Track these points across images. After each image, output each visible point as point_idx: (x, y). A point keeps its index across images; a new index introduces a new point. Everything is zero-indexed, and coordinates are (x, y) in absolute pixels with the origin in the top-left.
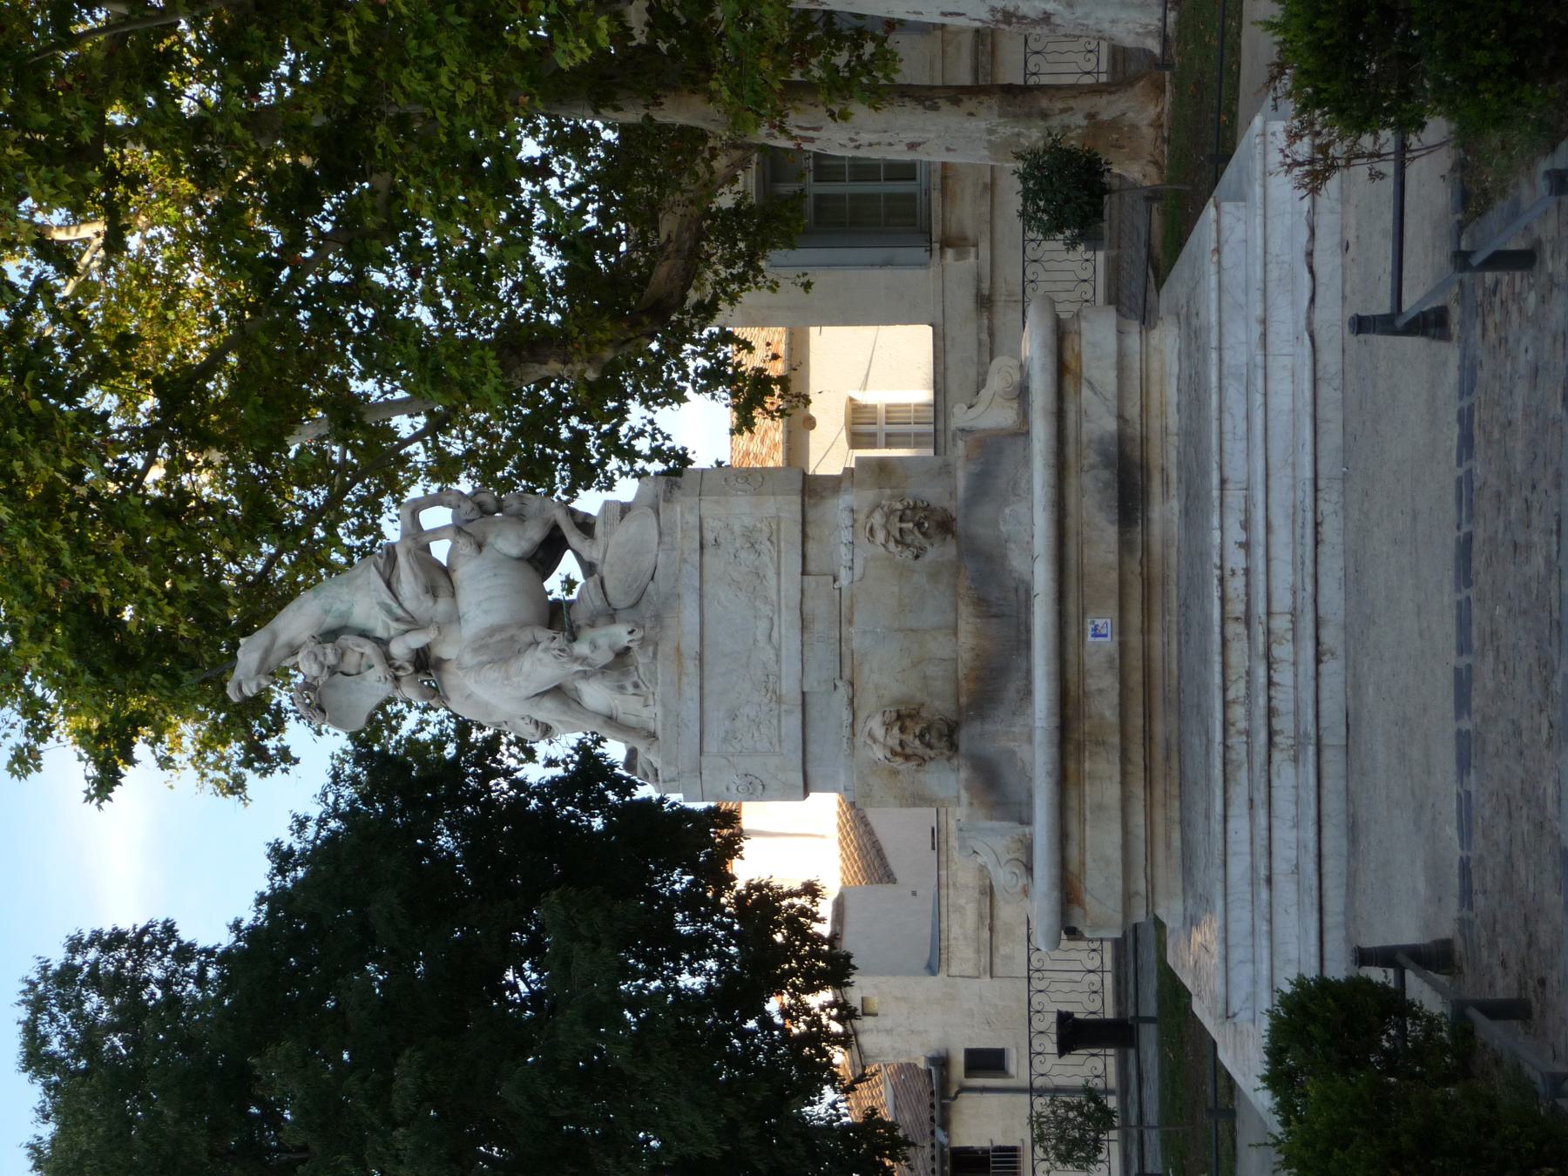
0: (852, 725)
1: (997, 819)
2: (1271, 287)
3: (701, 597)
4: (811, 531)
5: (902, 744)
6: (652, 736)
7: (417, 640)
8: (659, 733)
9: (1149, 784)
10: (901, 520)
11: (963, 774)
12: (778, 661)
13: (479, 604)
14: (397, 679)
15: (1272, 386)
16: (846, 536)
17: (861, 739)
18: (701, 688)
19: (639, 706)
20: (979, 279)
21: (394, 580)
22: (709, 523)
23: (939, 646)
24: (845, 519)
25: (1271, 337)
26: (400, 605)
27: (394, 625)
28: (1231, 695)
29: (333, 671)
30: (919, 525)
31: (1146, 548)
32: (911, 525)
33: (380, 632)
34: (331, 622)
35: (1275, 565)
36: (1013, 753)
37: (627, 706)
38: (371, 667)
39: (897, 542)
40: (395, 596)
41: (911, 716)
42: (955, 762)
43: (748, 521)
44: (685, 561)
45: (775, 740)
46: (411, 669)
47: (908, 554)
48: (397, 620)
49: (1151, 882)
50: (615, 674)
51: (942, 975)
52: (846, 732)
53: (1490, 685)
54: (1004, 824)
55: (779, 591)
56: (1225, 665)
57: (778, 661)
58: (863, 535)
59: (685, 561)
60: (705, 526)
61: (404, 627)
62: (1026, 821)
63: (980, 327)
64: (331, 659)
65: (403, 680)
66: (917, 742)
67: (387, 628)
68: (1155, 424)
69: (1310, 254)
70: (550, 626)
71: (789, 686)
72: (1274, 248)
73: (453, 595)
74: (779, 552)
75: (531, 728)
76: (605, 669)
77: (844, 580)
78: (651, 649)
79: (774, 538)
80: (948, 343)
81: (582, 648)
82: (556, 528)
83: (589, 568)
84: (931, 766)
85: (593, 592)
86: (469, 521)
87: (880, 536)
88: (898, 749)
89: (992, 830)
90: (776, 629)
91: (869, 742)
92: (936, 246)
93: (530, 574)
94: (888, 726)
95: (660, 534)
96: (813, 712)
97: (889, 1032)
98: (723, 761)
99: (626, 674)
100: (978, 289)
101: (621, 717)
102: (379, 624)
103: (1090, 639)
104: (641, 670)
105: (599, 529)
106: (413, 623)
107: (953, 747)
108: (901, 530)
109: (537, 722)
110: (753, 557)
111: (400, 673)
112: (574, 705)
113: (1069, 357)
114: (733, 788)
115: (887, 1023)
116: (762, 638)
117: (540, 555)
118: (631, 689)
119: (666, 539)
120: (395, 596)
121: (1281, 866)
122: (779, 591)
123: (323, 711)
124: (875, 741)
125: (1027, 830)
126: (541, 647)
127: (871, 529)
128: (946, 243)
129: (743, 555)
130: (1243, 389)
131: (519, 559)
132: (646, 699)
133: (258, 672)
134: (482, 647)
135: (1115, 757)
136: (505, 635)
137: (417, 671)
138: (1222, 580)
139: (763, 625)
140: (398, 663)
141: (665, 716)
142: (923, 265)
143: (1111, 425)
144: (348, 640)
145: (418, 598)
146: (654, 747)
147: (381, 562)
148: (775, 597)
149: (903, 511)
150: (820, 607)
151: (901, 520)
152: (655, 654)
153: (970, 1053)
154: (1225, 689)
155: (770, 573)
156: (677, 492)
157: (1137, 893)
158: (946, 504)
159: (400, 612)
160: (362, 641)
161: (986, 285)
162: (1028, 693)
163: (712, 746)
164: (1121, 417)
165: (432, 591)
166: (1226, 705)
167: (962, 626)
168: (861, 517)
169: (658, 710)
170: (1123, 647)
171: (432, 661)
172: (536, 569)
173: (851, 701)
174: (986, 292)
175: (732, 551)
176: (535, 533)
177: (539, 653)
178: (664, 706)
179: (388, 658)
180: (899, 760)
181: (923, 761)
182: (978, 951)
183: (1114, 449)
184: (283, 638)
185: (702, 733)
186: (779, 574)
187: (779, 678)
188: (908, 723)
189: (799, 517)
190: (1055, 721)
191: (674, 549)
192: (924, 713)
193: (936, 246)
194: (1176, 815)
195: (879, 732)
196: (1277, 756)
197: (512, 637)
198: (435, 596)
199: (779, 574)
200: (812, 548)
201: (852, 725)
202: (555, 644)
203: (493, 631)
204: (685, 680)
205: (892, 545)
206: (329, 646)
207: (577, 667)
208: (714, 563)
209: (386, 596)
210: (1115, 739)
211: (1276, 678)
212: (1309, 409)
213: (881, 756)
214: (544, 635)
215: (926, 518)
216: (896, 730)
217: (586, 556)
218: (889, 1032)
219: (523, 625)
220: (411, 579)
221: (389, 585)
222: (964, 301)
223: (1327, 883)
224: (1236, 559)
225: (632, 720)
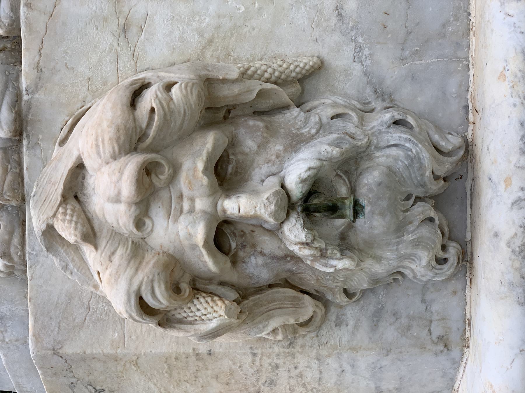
5: (224, 235)
88: (208, 263)
91: (67, 231)
94: (149, 150)
180: (212, 312)
195: (111, 188)
213: (117, 296)
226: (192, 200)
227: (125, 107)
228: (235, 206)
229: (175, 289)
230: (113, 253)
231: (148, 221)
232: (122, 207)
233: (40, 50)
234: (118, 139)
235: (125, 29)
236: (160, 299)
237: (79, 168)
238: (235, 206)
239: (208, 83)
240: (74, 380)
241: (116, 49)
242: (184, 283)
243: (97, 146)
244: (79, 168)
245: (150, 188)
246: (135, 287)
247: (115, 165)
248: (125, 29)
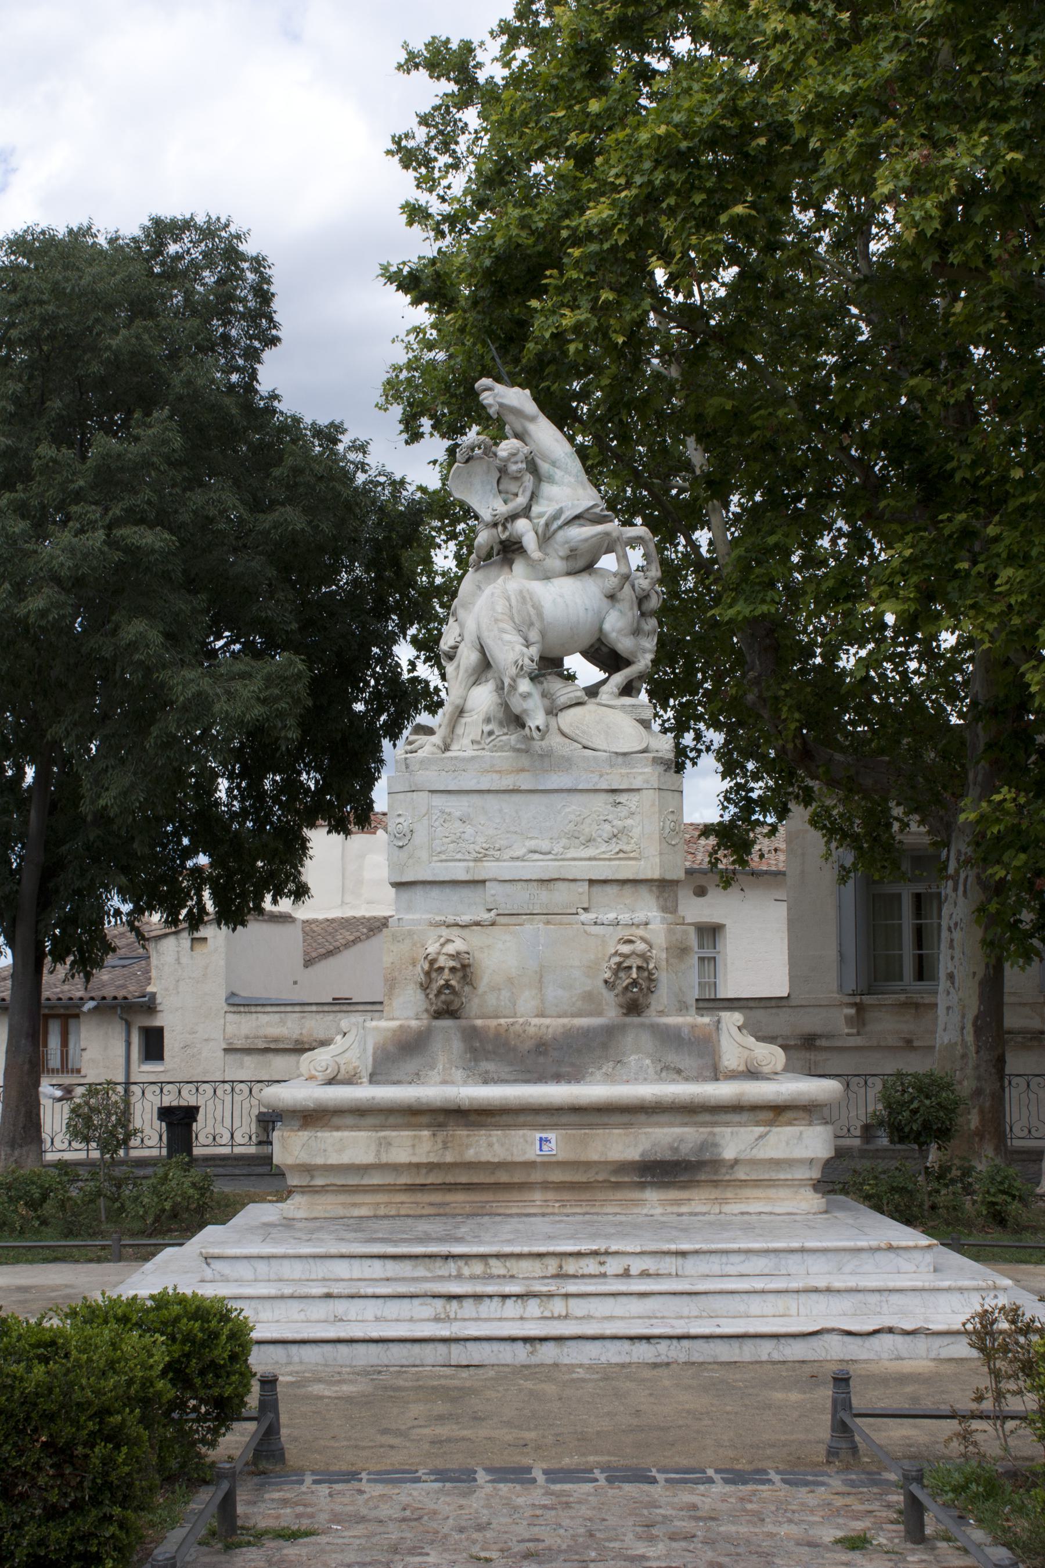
0: (457, 925)
1: (374, 1053)
2: (860, 1296)
3: (569, 791)
4: (628, 890)
5: (441, 969)
6: (447, 748)
7: (530, 542)
8: (448, 754)
9: (411, 1188)
10: (639, 968)
11: (414, 1023)
12: (512, 859)
13: (562, 596)
14: (495, 525)
15: (771, 1298)
16: (625, 917)
17: (445, 932)
18: (489, 791)
19: (471, 737)
20: (829, 1036)
21: (582, 521)
22: (635, 798)
23: (526, 1002)
24: (640, 916)
25: (814, 1296)
26: (560, 527)
27: (542, 521)
28: (493, 1262)
29: (503, 471)
30: (635, 983)
31: (617, 1186)
32: (634, 976)
33: (536, 509)
34: (544, 467)
35: (611, 1300)
36: (432, 1068)
37: (472, 726)
38: (506, 502)
39: (619, 964)
40: (569, 523)
42: (425, 1016)
43: (636, 832)
44: (601, 776)
45: (443, 857)
46: (503, 537)
47: (608, 975)
48: (547, 525)
49: (323, 1190)
50: (501, 715)
51: (226, 1008)
52: (451, 919)
53: (520, 1501)
54: (370, 1059)
55: (574, 859)
56: (520, 1256)
57: (512, 859)
58: (626, 933)
59: (601, 776)
60: (632, 794)
61: (540, 531)
62: (374, 1078)
63: (787, 1038)
64: (513, 468)
65: (494, 531)
66: (442, 982)
67: (540, 515)
68: (729, 1194)
69: (890, 1330)
70: (542, 658)
71: (488, 869)
72: (894, 1298)
73: (569, 574)
74: (610, 859)
75: (451, 642)
76: (506, 706)
77: (584, 917)
78: (523, 747)
79: (621, 855)
80: (774, 1011)
81: (524, 685)
82: (628, 663)
83: (592, 691)
84: (420, 996)
85: (572, 695)
86: (633, 586)
87: (625, 949)
88: (436, 966)
89: (365, 1050)
90: (541, 857)
91: (442, 940)
92: (857, 999)
93: (586, 642)
95: (625, 754)
96: (466, 892)
97: (178, 960)
98: (424, 811)
99: (501, 724)
100: (820, 1036)
101: (463, 721)
102: (543, 509)
103: (538, 1135)
104: (504, 738)
105: (627, 700)
106: (545, 538)
107: (438, 1015)
108: (630, 968)
109: (456, 647)
110: (605, 836)
111: (500, 528)
112: (473, 679)
113: (789, 1115)
114: (401, 820)
115: (184, 960)
116: (532, 844)
117: (604, 649)
118: (487, 728)
119: (620, 759)
120: (569, 523)
121: (340, 1307)
122: (574, 859)
123: (467, 461)
124: (442, 945)
125: (365, 1080)
126: (525, 649)
127: (631, 942)
128: (860, 1007)
129: (607, 827)
130: (766, 1271)
131: (601, 630)
132: (478, 743)
133: (501, 405)
134: (524, 598)
135: (433, 1158)
136: (534, 618)
137: (502, 542)
138: (595, 1253)
139: (545, 845)
140: (509, 525)
141: (463, 759)
142: (841, 987)
143: (729, 1153)
144: (529, 480)
145: (566, 542)
146: (435, 750)
147: (597, 510)
148: (569, 856)
149: (647, 969)
150: (561, 896)
151: (639, 968)
152: (518, 750)
153: (160, 1031)
154: (497, 1256)
155: (591, 852)
156: (661, 769)
157: (312, 1177)
158: (652, 1008)
159: (555, 526)
160: (528, 494)
161: (823, 1043)
162: (679, 1073)
163: (438, 801)
164: (736, 1162)
165: (572, 554)
166: (483, 1257)
167: (547, 1021)
168: (641, 932)
169: (470, 753)
170: (530, 1165)
171: (509, 556)
172: (592, 646)
173: (477, 924)
174: (818, 1043)
175: (610, 817)
176: (624, 644)
177: (519, 648)
178: (473, 758)
179: (513, 517)
180: (426, 966)
181: (425, 987)
182: (247, 1037)
183: (707, 1156)
184: (532, 427)
185: (449, 792)
186: (590, 859)
187: (498, 860)
188: (460, 974)
189: (641, 876)
190: (466, 1105)
191: (611, 766)
192: (467, 988)
193: (857, 999)
194: (382, 1212)
195: (450, 949)
196: (439, 1303)
197: (532, 624)
198: (568, 558)
199: (590, 859)
200: (612, 890)
201: (457, 925)
202: (527, 661)
203: (538, 608)
204: (496, 776)
205: (617, 959)
206: (524, 466)
207: (507, 681)
208: (600, 804)
209: (568, 514)
210: (449, 1158)
211: (509, 1302)
212: (752, 1330)
213: (429, 950)
214: (534, 651)
215: (641, 989)
216: (452, 964)
217: (604, 689)
218: (178, 960)
219: (543, 634)
220: (583, 537)
221: (577, 517)
222: (811, 1023)
223: (327, 1348)
224: (614, 1266)
225: (459, 730)
228: (447, 971)
238: (447, 971)
239: (469, 966)
245: (451, 956)
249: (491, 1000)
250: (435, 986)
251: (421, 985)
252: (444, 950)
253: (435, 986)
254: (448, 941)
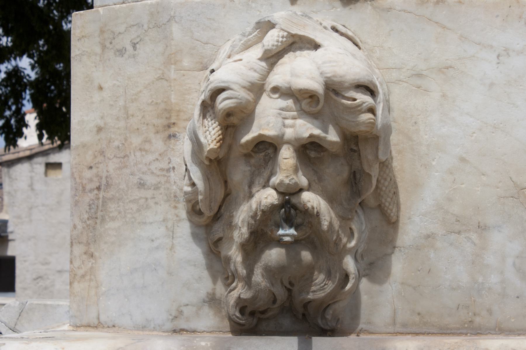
5: (266, 149)
41: (355, 181)
66: (268, 197)
84: (188, 251)
124: (272, 58)
181: (209, 218)
188: (336, 173)
195: (301, 71)
216: (305, 128)
226: (292, 126)
227: (356, 81)
228: (287, 156)
229: (229, 114)
230: (255, 71)
231: (277, 96)
232: (288, 78)
233: (404, 11)
234: (334, 76)
235: (419, 75)
236: (223, 103)
237: (316, 46)
238: (287, 156)
240: (146, 27)
241: (404, 68)
242: (234, 122)
243: (330, 62)
244: (316, 46)
246: (233, 86)
247: (316, 74)
248: (419, 75)
249: (452, 266)
250: (242, 216)
251: (194, 211)
252: (281, 76)
253: (242, 216)
254: (297, 43)
